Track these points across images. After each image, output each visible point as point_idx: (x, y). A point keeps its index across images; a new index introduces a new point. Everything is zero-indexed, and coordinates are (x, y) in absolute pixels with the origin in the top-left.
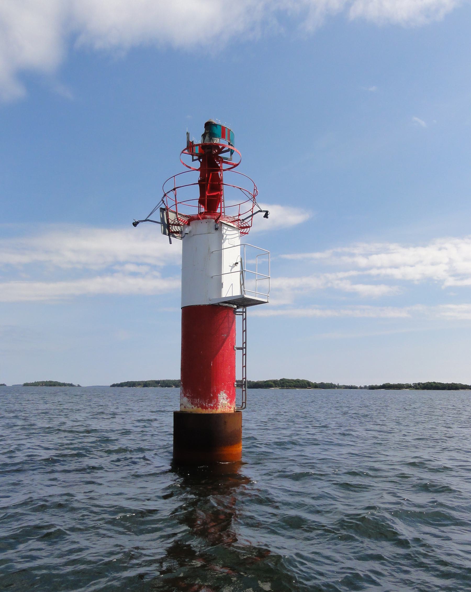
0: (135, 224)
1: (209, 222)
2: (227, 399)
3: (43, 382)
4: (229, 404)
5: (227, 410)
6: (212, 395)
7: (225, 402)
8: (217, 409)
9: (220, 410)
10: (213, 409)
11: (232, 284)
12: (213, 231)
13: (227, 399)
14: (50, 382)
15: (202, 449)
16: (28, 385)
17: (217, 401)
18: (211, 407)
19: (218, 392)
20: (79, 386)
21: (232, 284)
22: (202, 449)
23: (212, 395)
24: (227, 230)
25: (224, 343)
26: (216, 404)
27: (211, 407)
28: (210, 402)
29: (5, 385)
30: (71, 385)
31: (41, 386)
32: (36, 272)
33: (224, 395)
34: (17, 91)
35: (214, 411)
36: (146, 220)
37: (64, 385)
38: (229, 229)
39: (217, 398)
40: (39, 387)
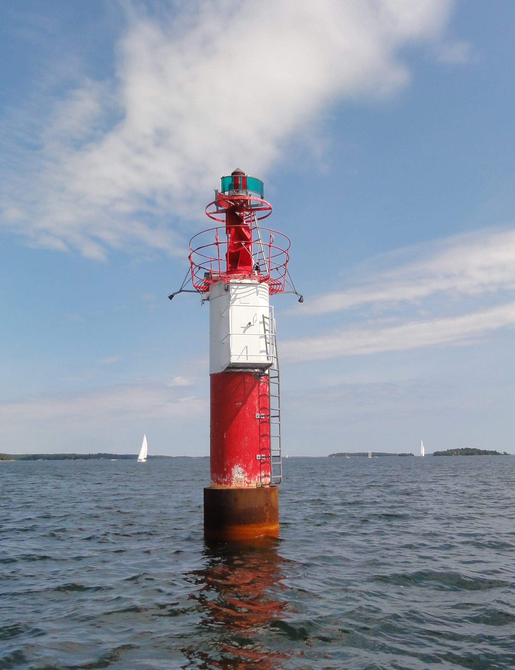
0: (171, 297)
1: (220, 284)
2: (243, 473)
3: (458, 450)
4: (246, 479)
5: (244, 486)
6: (225, 470)
7: (241, 477)
8: (231, 484)
9: (234, 485)
10: (227, 484)
11: (247, 347)
12: (224, 292)
13: (243, 473)
14: (467, 449)
15: (229, 527)
16: (439, 455)
17: (231, 476)
18: (225, 483)
19: (232, 465)
20: (505, 454)
21: (247, 347)
22: (229, 527)
23: (225, 470)
24: (236, 289)
25: (238, 412)
26: (229, 479)
27: (225, 483)
28: (224, 477)
29: (413, 455)
30: (495, 453)
31: (455, 455)
32: (440, 306)
33: (240, 469)
34: (399, 77)
35: (228, 487)
36: (181, 291)
37: (486, 453)
38: (240, 287)
39: (231, 472)
40: (453, 458)
